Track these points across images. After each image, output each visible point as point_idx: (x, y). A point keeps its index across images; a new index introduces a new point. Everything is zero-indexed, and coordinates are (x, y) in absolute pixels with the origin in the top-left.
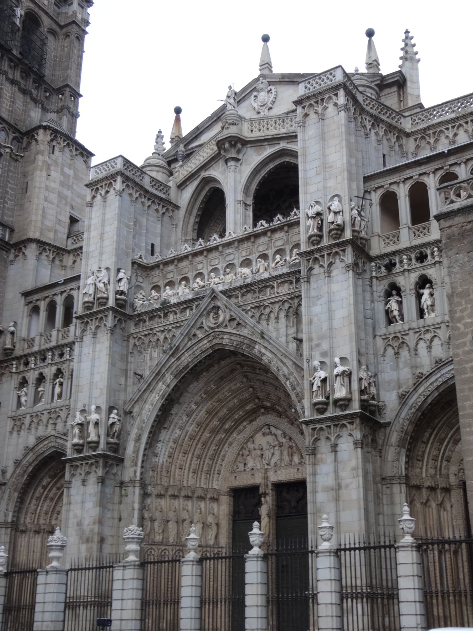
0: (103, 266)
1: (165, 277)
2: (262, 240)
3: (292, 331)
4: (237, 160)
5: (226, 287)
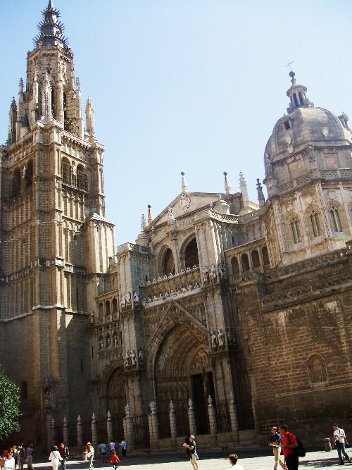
0: (128, 291)
1: (153, 292)
2: (189, 276)
4: (176, 240)
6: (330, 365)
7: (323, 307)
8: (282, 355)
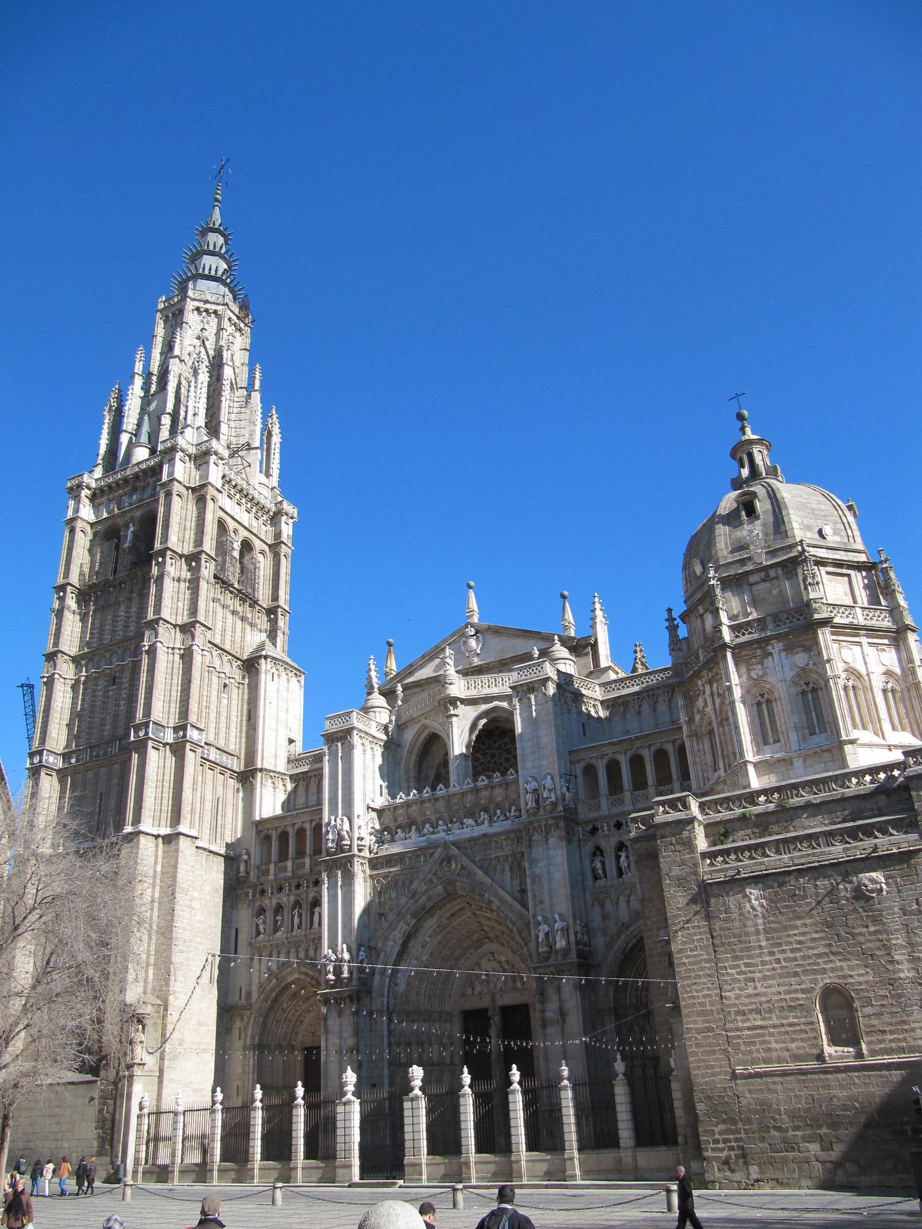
3: (516, 882)
5: (456, 838)
6: (868, 1010)
7: (851, 882)
8: (753, 980)
